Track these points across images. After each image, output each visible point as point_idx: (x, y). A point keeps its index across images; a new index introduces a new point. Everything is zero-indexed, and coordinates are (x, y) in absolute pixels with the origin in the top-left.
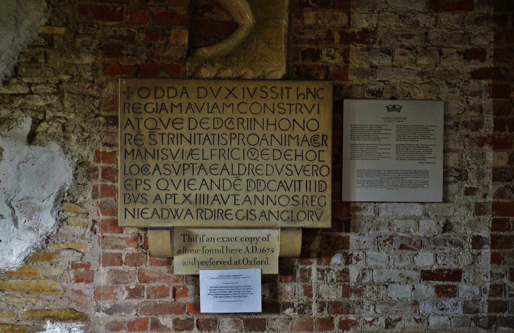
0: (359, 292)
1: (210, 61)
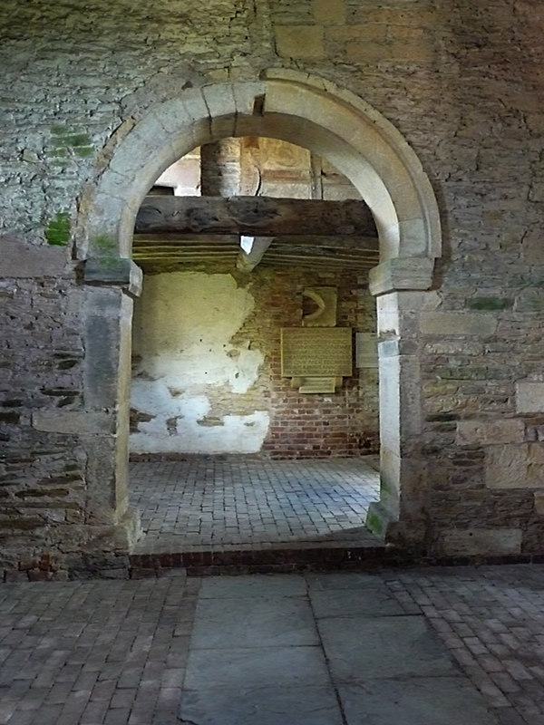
0: (363, 400)
1: (311, 321)
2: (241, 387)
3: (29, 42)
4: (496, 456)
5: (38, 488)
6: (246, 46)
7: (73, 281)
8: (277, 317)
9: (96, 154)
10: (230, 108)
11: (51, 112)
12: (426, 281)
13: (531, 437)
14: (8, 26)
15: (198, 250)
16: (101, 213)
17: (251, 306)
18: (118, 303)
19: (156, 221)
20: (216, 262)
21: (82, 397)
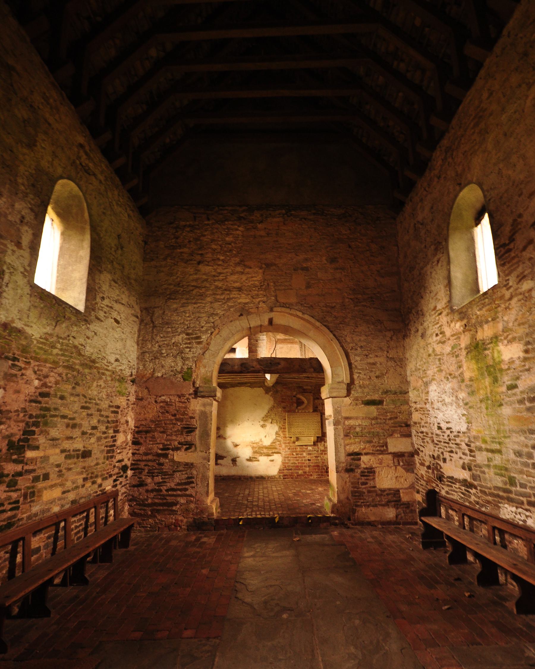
2: (267, 442)
3: (178, 301)
4: (380, 473)
5: (175, 487)
6: (265, 299)
7: (193, 396)
8: (284, 408)
9: (204, 343)
10: (259, 323)
11: (186, 327)
12: (344, 392)
13: (396, 464)
14: (170, 294)
15: (246, 378)
16: (205, 367)
17: (272, 403)
18: (211, 405)
19: (229, 368)
20: (255, 383)
21: (195, 446)
